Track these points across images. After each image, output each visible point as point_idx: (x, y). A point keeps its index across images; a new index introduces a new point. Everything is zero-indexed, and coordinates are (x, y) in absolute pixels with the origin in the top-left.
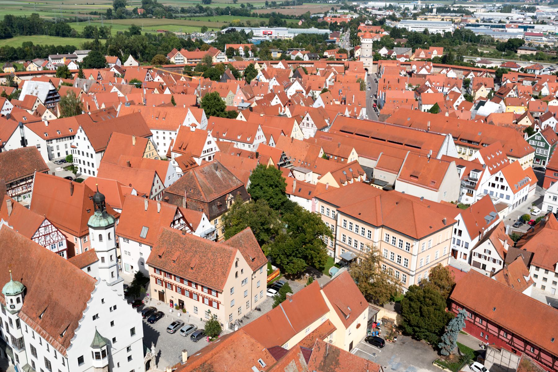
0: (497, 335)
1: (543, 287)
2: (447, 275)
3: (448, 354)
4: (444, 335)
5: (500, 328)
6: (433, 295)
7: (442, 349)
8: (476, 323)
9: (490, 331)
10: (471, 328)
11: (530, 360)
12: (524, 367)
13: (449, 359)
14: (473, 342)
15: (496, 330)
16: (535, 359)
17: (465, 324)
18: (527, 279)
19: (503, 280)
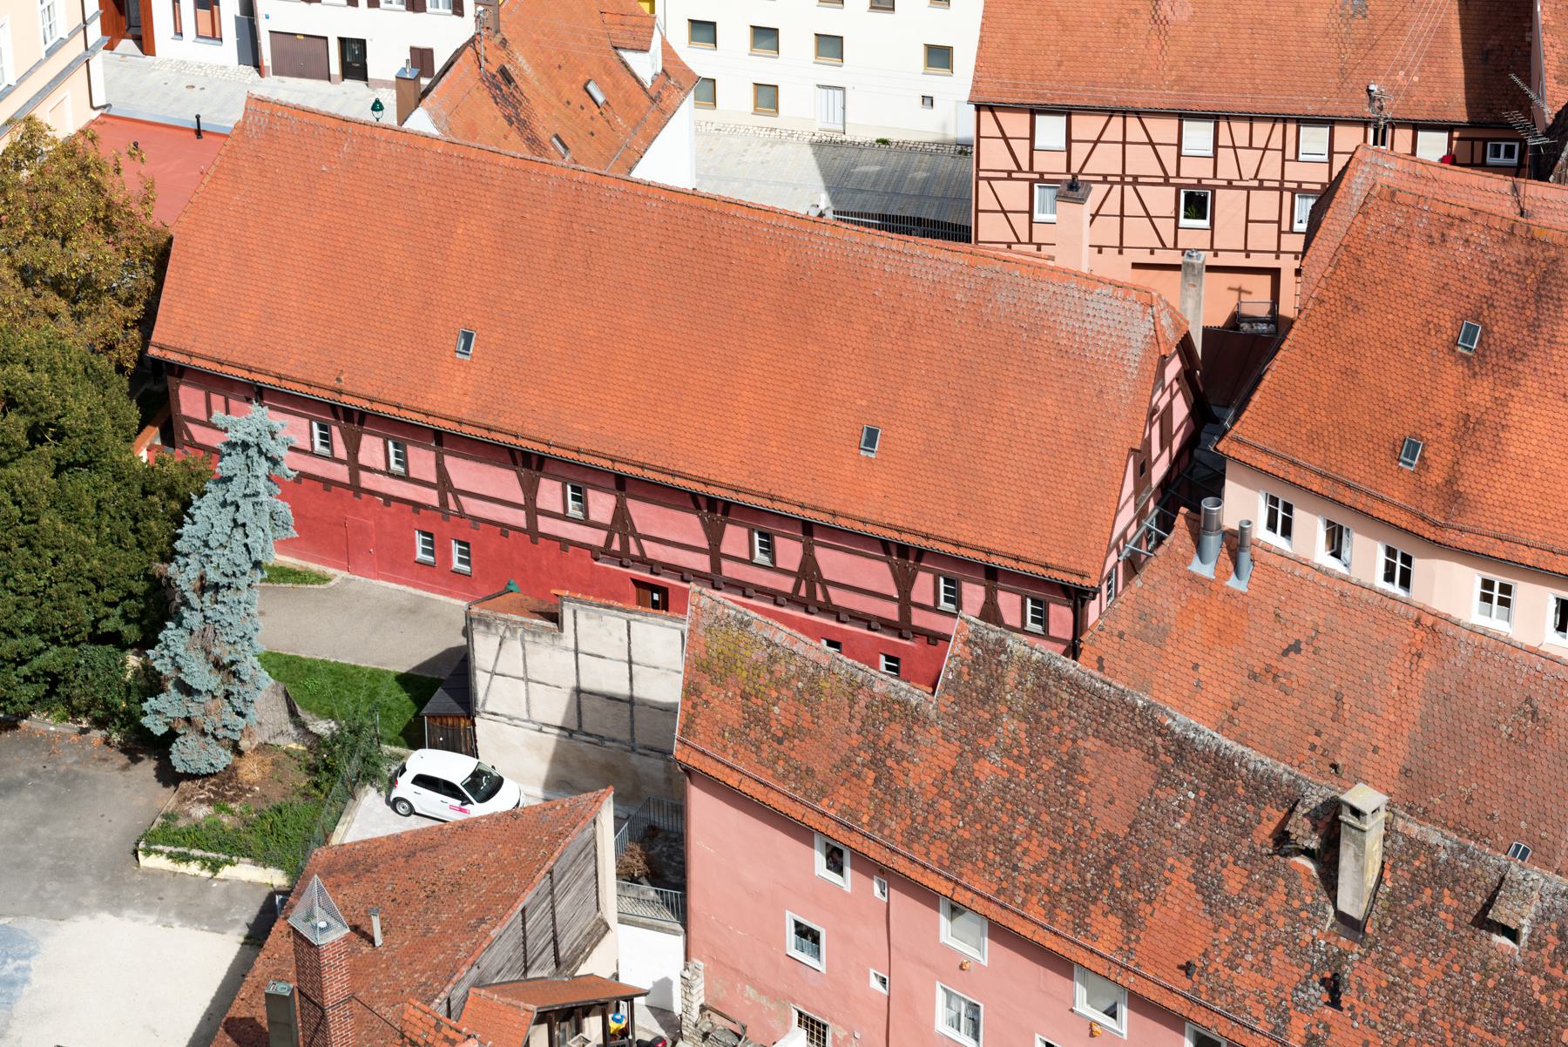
0: (518, 518)
1: (767, 96)
2: (97, 188)
3: (224, 758)
4: (170, 632)
5: (529, 464)
6: (19, 371)
7: (172, 735)
8: (367, 481)
9: (473, 507)
10: (336, 521)
11: (744, 624)
12: (719, 680)
13: (241, 791)
14: (377, 623)
15: (505, 483)
16: (793, 600)
17: (284, 508)
18: (645, 66)
19: (489, 114)
